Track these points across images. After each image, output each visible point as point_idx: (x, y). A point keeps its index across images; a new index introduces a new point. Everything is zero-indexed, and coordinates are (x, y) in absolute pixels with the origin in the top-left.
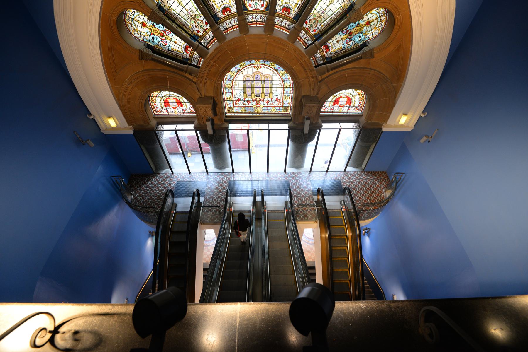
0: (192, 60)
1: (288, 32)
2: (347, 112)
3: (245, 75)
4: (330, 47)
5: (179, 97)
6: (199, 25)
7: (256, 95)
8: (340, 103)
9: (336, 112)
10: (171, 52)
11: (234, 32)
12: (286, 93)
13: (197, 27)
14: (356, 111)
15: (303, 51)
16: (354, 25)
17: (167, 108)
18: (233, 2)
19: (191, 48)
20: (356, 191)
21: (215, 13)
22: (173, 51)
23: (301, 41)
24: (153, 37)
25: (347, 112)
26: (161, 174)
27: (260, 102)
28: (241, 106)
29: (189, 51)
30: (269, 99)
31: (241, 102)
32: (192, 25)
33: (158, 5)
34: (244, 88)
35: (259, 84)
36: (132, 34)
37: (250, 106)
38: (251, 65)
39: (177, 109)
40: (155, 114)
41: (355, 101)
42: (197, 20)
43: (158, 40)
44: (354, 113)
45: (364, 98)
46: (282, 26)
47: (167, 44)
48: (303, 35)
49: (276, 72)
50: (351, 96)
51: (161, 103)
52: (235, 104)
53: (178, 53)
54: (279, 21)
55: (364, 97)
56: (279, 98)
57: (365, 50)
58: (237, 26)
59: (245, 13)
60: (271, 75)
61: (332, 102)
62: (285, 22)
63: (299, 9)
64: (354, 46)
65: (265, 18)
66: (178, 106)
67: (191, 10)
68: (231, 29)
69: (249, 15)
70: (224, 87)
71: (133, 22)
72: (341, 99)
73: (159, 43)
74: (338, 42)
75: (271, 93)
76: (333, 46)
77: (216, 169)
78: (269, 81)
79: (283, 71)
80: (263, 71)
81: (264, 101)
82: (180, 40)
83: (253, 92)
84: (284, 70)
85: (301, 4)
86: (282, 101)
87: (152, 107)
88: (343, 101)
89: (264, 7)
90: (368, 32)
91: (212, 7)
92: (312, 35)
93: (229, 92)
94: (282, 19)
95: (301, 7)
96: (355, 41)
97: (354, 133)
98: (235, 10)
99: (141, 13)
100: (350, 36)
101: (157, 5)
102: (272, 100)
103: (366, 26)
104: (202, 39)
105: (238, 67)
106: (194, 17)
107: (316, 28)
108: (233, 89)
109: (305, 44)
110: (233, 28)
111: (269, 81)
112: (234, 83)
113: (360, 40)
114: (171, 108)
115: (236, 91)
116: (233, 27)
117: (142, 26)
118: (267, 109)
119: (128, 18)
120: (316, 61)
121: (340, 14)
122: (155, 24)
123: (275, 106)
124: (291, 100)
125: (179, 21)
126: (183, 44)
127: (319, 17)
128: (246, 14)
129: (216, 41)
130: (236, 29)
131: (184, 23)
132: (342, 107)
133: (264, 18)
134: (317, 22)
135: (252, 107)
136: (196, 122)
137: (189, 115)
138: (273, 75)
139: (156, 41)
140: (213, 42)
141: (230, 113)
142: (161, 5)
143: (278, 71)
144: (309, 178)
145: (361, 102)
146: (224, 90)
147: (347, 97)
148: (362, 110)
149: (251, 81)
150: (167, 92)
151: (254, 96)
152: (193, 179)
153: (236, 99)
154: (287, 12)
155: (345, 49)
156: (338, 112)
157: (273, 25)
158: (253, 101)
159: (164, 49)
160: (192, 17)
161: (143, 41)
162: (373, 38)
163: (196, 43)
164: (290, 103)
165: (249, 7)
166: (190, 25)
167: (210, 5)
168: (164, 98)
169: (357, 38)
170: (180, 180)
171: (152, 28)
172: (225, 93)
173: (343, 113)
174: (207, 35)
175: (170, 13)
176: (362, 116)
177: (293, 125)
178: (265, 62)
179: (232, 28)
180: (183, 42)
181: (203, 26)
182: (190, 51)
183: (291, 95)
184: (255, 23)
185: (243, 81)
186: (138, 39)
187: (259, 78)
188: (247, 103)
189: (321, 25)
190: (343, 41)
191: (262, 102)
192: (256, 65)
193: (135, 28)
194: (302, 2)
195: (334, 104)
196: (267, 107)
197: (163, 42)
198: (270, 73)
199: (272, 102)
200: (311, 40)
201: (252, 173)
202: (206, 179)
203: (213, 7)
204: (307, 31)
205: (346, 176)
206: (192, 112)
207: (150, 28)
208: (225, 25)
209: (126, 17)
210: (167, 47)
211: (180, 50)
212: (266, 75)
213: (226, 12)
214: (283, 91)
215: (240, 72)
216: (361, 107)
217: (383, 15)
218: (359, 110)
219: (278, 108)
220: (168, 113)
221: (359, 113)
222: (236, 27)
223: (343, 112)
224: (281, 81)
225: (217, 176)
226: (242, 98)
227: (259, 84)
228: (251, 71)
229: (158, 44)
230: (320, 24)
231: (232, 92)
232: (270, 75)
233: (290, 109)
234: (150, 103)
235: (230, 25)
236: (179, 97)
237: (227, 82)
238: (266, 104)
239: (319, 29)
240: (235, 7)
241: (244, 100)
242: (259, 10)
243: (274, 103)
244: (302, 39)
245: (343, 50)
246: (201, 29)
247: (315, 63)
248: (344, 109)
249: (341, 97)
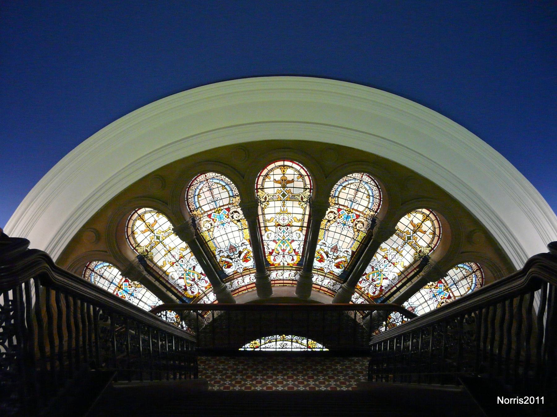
48: (357, 298)
58: (254, 285)
59: (267, 268)
65: (298, 277)
69: (272, 272)
110: (247, 289)
128: (268, 271)
133: (295, 275)
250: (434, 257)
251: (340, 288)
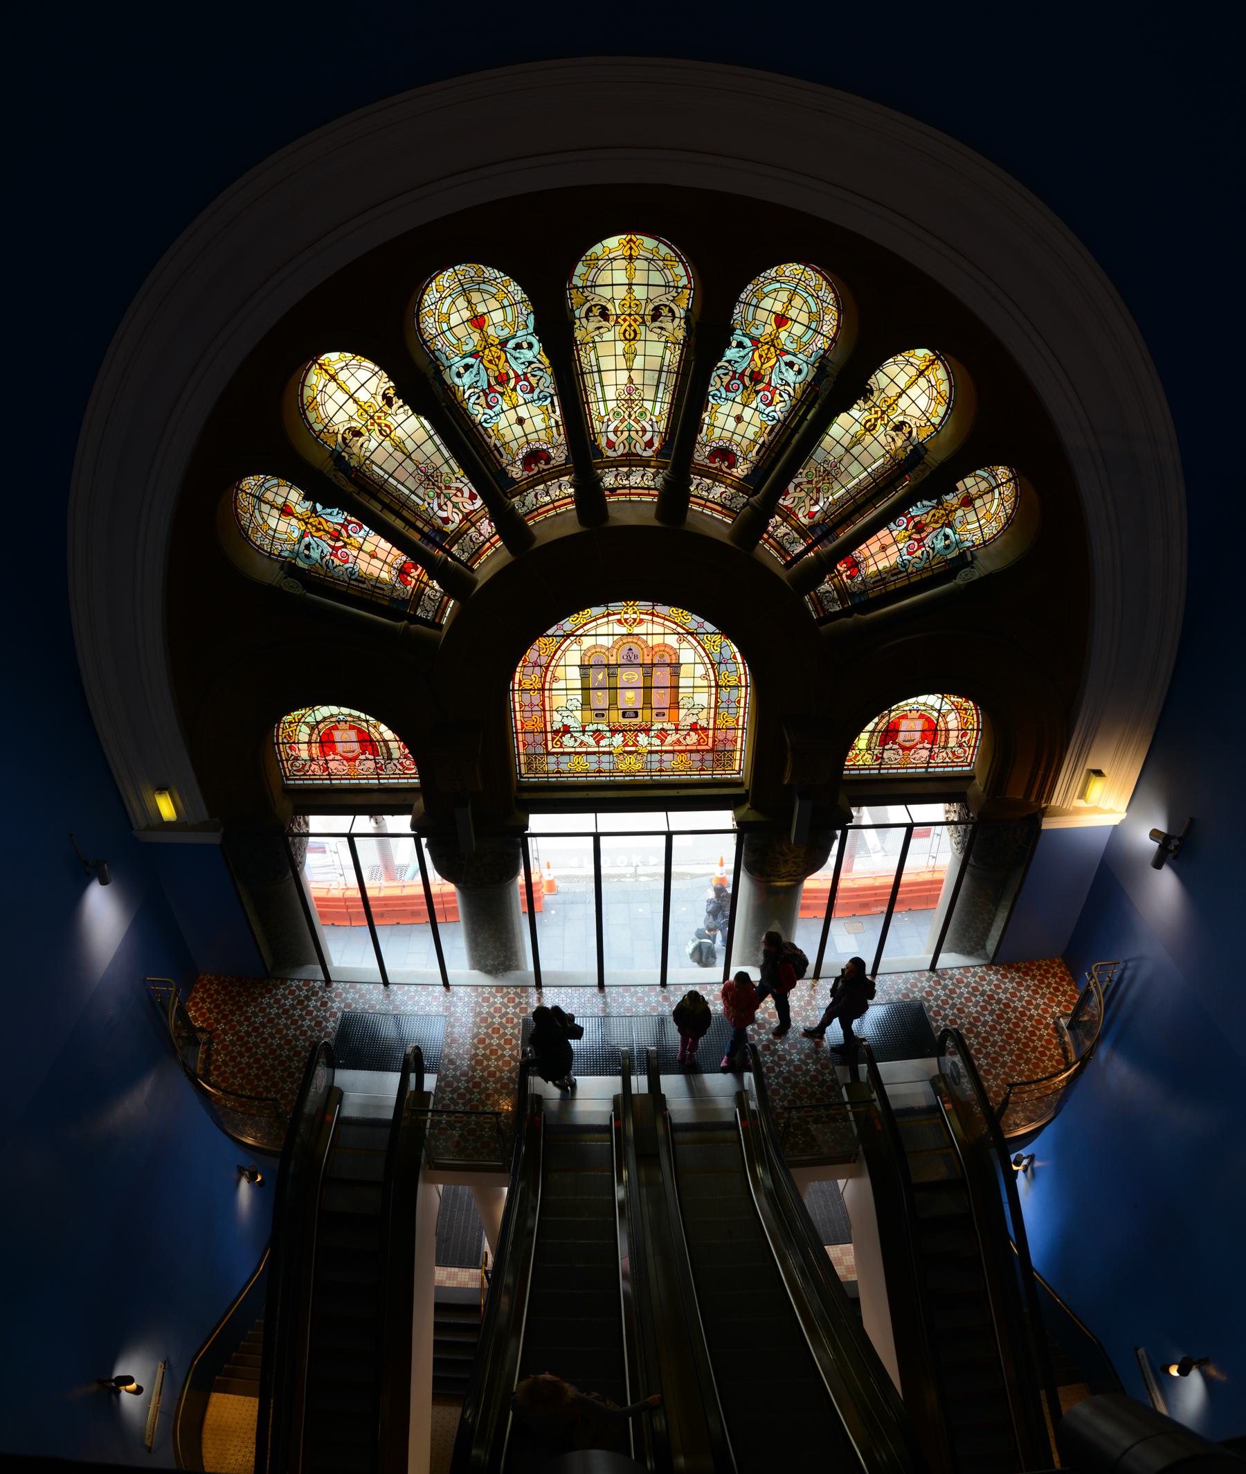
0: (418, 605)
1: (729, 516)
2: (927, 768)
3: (589, 649)
4: (859, 562)
5: (367, 721)
6: (448, 503)
7: (624, 715)
8: (901, 737)
9: (891, 768)
10: (356, 584)
11: (558, 517)
12: (724, 705)
13: (444, 507)
14: (953, 762)
15: (783, 575)
16: (929, 504)
17: (327, 758)
18: (559, 435)
19: (420, 568)
20: (977, 1035)
21: (501, 466)
22: (363, 579)
23: (770, 544)
24: (310, 544)
25: (927, 768)
26: (292, 980)
27: (637, 736)
28: (573, 750)
29: (411, 577)
30: (666, 726)
31: (572, 736)
32: (429, 504)
33: (335, 454)
34: (582, 689)
35: (634, 676)
36: (252, 537)
37: (601, 749)
38: (608, 615)
39: (357, 762)
40: (288, 779)
41: (947, 730)
42: (443, 488)
43: (322, 551)
44: (946, 769)
45: (975, 720)
46: (711, 502)
47: (346, 562)
48: (776, 527)
49: (689, 637)
50: (936, 714)
51: (309, 743)
52: (550, 744)
53: (378, 585)
54: (700, 487)
55: (975, 716)
56: (703, 723)
57: (961, 579)
60: (676, 646)
61: (876, 734)
62: (718, 491)
63: (761, 454)
64: (933, 563)
66: (363, 753)
67: (428, 461)
68: (549, 510)
70: (516, 687)
71: (257, 507)
72: (904, 725)
73: (325, 560)
74: (884, 548)
75: (675, 705)
76: (871, 561)
77: (476, 972)
78: (669, 665)
79: (713, 633)
80: (647, 634)
81: (652, 733)
82: (388, 546)
83: (613, 703)
84: (717, 631)
85: (767, 442)
86: (711, 733)
87: (281, 755)
88: (911, 729)
89: (654, 448)
90: (968, 523)
91: (492, 452)
92: (805, 525)
93: (531, 704)
94: (709, 481)
95: (767, 449)
96: (933, 549)
97: (951, 836)
98: (564, 457)
99: (282, 482)
100: (919, 532)
101: (330, 456)
102: (677, 730)
103: (963, 508)
104: (456, 542)
105: (568, 624)
106: (437, 481)
107: (816, 508)
108: (547, 693)
109: (782, 551)
111: (669, 665)
112: (549, 674)
113: (947, 547)
114: (340, 758)
115: (559, 700)
116: (556, 504)
117: (280, 516)
118: (661, 761)
119: (244, 496)
120: (821, 602)
121: (887, 471)
122: (319, 507)
123: (688, 748)
124: (743, 729)
125: (391, 495)
126: (398, 557)
127: (824, 479)
129: (500, 544)
130: (563, 509)
131: (403, 499)
132: (910, 749)
133: (654, 478)
134: (818, 490)
135: (610, 753)
136: (419, 804)
137: (396, 781)
138: (682, 646)
139: (315, 554)
140: (488, 549)
141: (533, 775)
142: (343, 454)
143: (697, 634)
144: (814, 1003)
145: (964, 735)
146: (516, 696)
147: (921, 716)
148: (972, 759)
149: (608, 666)
150: (334, 710)
151: (615, 716)
152: (396, 1007)
153: (557, 726)
154: (726, 463)
155: (907, 570)
156: (897, 768)
157: (686, 496)
158: (614, 732)
159: (336, 576)
160: (430, 480)
161: (279, 556)
162: (985, 542)
163: (438, 553)
164: (739, 740)
165: (607, 449)
166: (420, 502)
167: (488, 446)
168: (321, 726)
169: (939, 541)
170: (354, 1006)
171: (308, 518)
172: (517, 708)
173: (913, 770)
174: (473, 529)
175: (367, 474)
176: (973, 778)
177: (753, 816)
178: (654, 605)
179: (551, 506)
180: (395, 551)
181: (460, 504)
182: (416, 577)
183: (742, 713)
184: (627, 491)
185: (582, 666)
186: (266, 551)
187: (636, 657)
188: (591, 741)
189: (830, 500)
190: (900, 546)
191: (642, 739)
192: (626, 616)
193: (261, 522)
194: (771, 438)
195: (883, 743)
196: (661, 751)
197: (336, 555)
198: (672, 640)
199: (678, 736)
200: (802, 541)
201: (607, 989)
202: (441, 1009)
203: (496, 452)
204: (788, 515)
205: (939, 987)
206: (406, 771)
207: (303, 520)
208: (530, 497)
209: (240, 495)
210: (347, 569)
211: (384, 575)
212: (659, 645)
213: (536, 465)
214: (716, 698)
215: (572, 638)
216: (967, 749)
217: (1006, 483)
218: (961, 757)
219: (696, 757)
220: (329, 774)
221: (965, 769)
222: (565, 504)
223: (912, 768)
224: (709, 666)
225: (480, 1000)
226: (573, 723)
227: (634, 676)
228: (608, 635)
229: (319, 561)
230: (828, 498)
231: (543, 705)
232: (672, 648)
233: (738, 757)
234: (278, 744)
235: (547, 499)
236: (367, 721)
237: (529, 670)
238: (658, 742)
239: (825, 512)
240: (564, 448)
242: (637, 455)
243: (685, 739)
244: (774, 539)
245: (901, 572)
246: (455, 515)
247: (816, 611)
248: (917, 756)
249: (905, 717)
250: (936, 457)
251: (745, 505)
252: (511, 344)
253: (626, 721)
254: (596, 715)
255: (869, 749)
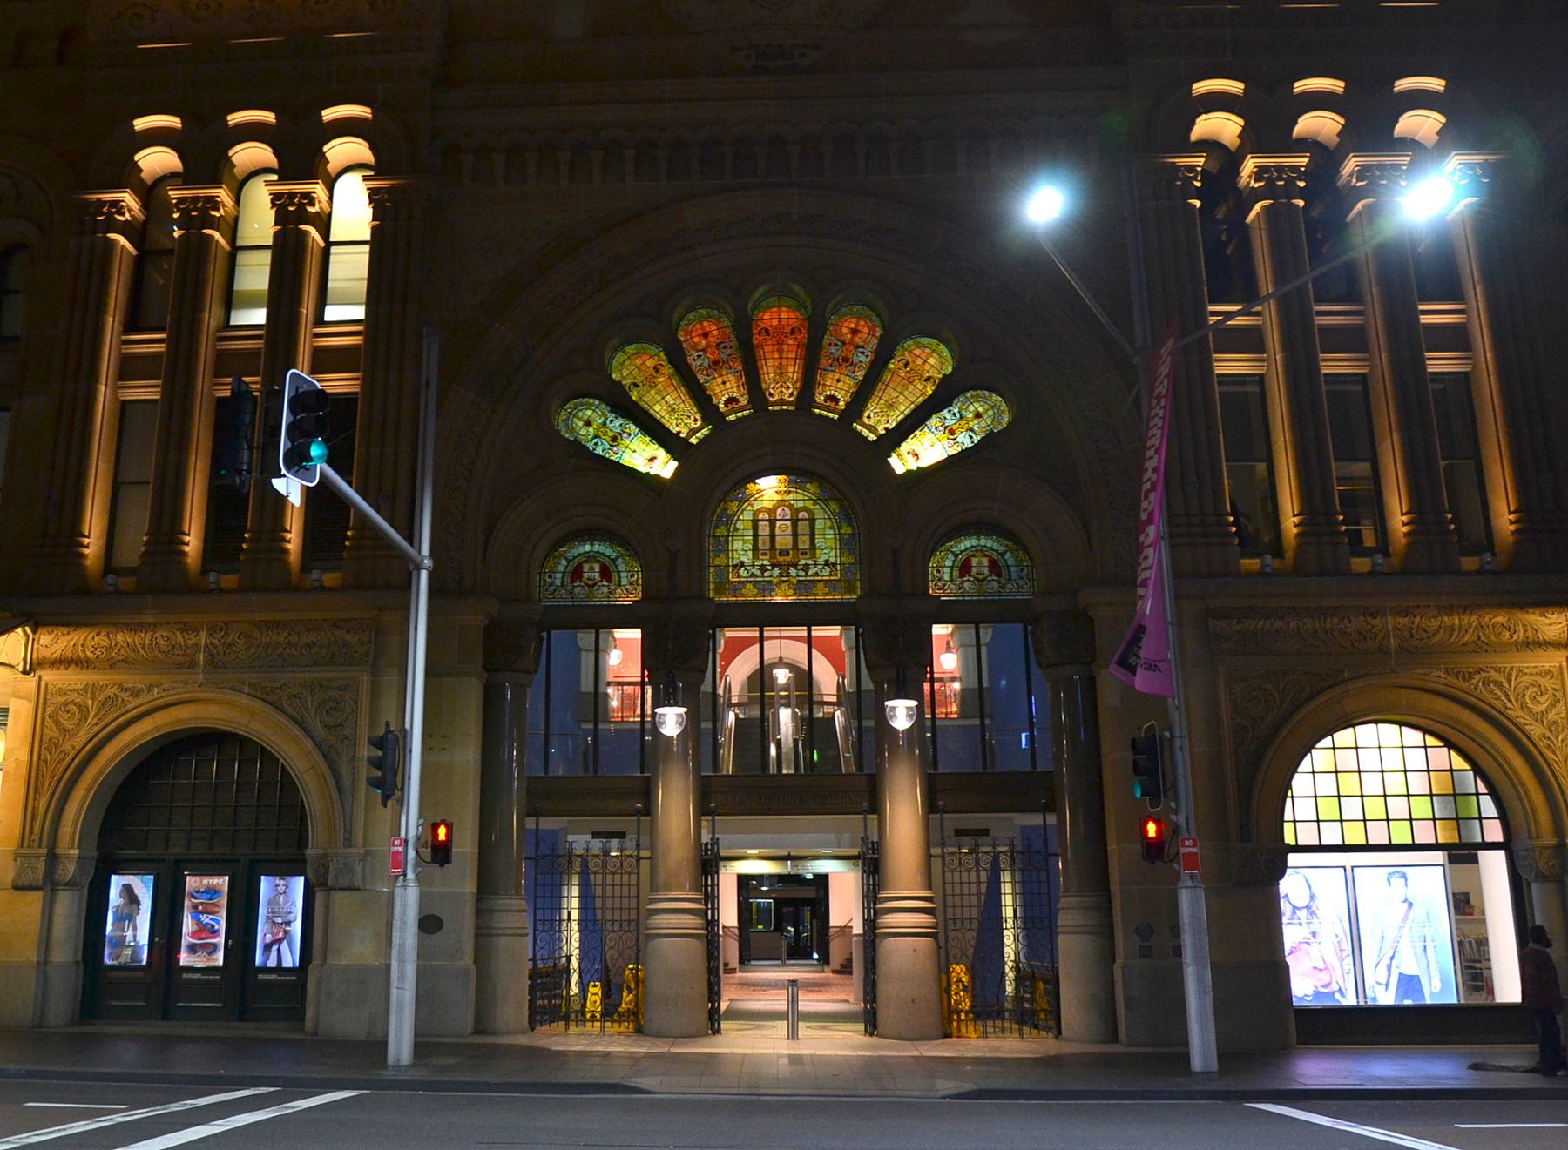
56: (832, 560)
86: (838, 567)
102: (815, 565)
158: (773, 566)
188: (759, 573)
191: (793, 571)
226: (747, 559)
238: (803, 574)
241: (753, 566)
249: (973, 556)
252: (722, 346)
253: (781, 559)
254: (762, 555)
255: (951, 580)
